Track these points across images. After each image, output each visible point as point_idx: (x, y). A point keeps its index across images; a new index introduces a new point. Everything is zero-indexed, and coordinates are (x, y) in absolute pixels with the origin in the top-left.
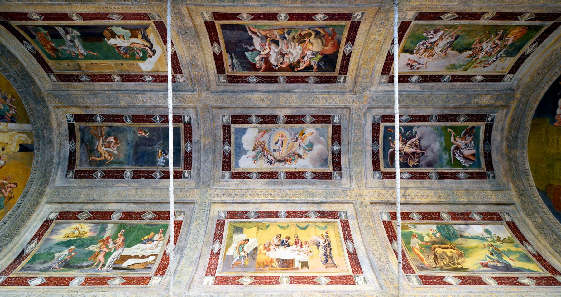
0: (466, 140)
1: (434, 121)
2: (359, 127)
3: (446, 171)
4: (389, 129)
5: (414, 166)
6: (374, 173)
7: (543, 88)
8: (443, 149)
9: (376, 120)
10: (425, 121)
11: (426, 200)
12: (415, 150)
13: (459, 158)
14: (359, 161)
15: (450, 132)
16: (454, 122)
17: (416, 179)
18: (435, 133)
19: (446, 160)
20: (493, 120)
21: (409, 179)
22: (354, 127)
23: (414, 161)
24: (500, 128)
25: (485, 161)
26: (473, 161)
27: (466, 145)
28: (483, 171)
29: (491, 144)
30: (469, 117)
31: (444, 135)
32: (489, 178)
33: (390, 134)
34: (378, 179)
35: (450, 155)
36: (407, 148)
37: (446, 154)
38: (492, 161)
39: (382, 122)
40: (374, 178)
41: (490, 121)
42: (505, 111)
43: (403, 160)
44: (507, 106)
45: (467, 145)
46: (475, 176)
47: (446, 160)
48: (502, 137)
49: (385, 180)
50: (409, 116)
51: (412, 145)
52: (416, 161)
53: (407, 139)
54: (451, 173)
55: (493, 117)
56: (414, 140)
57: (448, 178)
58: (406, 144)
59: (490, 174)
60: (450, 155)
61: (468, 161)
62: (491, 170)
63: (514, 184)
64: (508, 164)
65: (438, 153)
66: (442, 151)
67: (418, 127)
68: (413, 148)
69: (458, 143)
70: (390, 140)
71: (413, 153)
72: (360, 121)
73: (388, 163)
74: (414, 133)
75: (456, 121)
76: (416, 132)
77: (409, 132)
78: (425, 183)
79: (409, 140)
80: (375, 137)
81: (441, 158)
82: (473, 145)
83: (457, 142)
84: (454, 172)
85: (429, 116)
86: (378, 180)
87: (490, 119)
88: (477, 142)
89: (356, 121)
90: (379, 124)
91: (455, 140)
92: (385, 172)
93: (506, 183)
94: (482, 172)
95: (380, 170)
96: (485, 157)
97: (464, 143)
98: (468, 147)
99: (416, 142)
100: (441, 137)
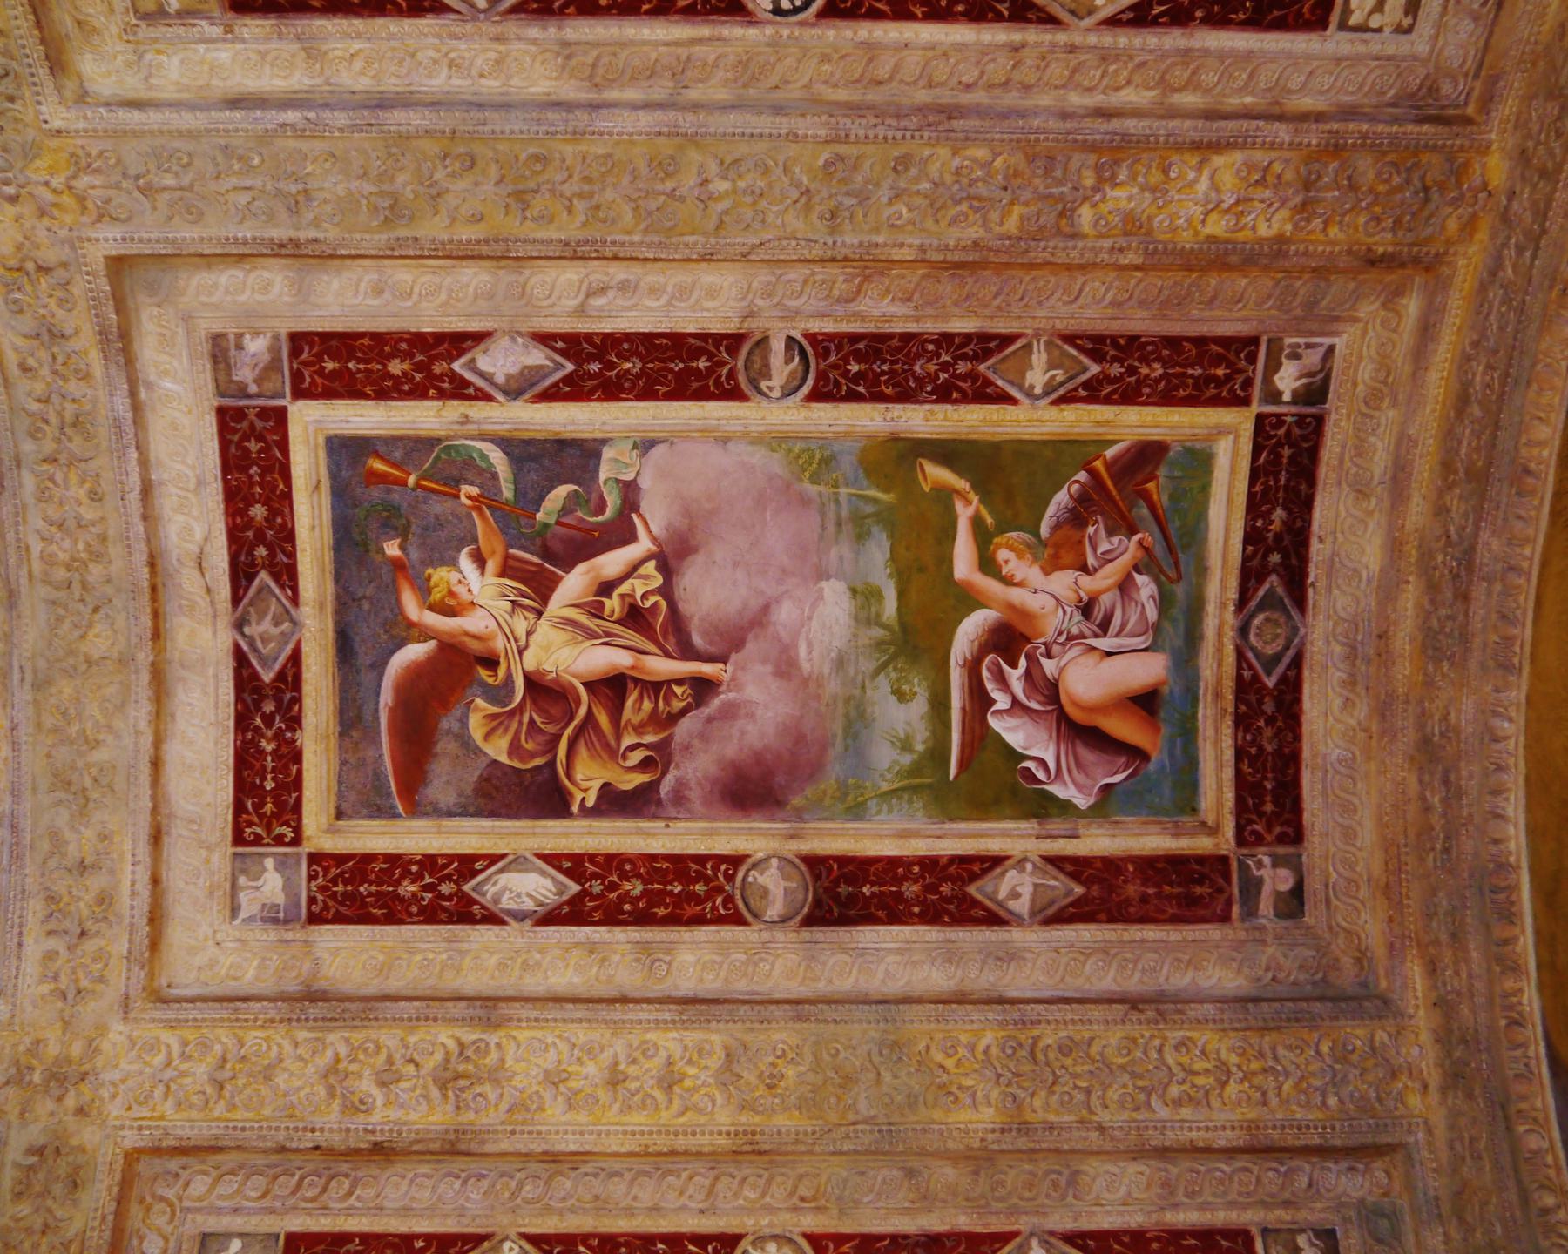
0: (1084, 568)
1: (788, 392)
2: (76, 445)
3: (889, 849)
4: (378, 465)
5: (614, 803)
6: (242, 867)
8: (879, 645)
9: (245, 374)
10: (702, 395)
12: (620, 659)
13: (1014, 732)
14: (100, 756)
15: (945, 496)
16: (965, 399)
17: (612, 917)
18: (805, 501)
19: (906, 745)
20: (1315, 392)
21: (551, 918)
22: (27, 447)
23: (613, 754)
24: (1380, 463)
25: (1240, 754)
26: (1136, 754)
27: (1086, 609)
28: (1203, 844)
29: (1301, 603)
30: (1096, 355)
31: (885, 517)
32: (1251, 912)
33: (393, 510)
34: (273, 917)
35: (939, 704)
36: (560, 636)
37: (901, 696)
38: (1294, 759)
39: (299, 393)
40: (235, 911)
41: (1298, 398)
43: (515, 749)
45: (1098, 614)
46: (1132, 890)
47: (906, 745)
48: (1395, 547)
49: (330, 937)
50: (544, 339)
51: (596, 611)
52: (636, 757)
53: (547, 554)
54: (930, 864)
55: (1313, 359)
56: (612, 562)
57: (892, 912)
58: (544, 599)
59: (1266, 873)
60: (939, 704)
61: (1087, 755)
62: (1282, 839)
65: (833, 687)
66: (868, 665)
67: (645, 446)
68: (608, 640)
69: (1016, 595)
70: (398, 565)
71: (612, 687)
72: (74, 387)
73: (378, 775)
74: (613, 501)
75: (985, 394)
76: (630, 492)
77: (562, 491)
78: (686, 957)
79: (569, 566)
80: (260, 538)
81: (857, 720)
82: (1152, 613)
83: (1008, 581)
84: (954, 859)
85: (733, 341)
86: (272, 934)
87: (1287, 380)
88: (1180, 590)
89: (39, 388)
90: (280, 417)
91: (987, 564)
92: (340, 859)
93: (1380, 952)
94: (1201, 859)
95: (296, 841)
96: (1241, 722)
97: (1067, 595)
98: (1104, 627)
99: (636, 587)
100: (861, 536)
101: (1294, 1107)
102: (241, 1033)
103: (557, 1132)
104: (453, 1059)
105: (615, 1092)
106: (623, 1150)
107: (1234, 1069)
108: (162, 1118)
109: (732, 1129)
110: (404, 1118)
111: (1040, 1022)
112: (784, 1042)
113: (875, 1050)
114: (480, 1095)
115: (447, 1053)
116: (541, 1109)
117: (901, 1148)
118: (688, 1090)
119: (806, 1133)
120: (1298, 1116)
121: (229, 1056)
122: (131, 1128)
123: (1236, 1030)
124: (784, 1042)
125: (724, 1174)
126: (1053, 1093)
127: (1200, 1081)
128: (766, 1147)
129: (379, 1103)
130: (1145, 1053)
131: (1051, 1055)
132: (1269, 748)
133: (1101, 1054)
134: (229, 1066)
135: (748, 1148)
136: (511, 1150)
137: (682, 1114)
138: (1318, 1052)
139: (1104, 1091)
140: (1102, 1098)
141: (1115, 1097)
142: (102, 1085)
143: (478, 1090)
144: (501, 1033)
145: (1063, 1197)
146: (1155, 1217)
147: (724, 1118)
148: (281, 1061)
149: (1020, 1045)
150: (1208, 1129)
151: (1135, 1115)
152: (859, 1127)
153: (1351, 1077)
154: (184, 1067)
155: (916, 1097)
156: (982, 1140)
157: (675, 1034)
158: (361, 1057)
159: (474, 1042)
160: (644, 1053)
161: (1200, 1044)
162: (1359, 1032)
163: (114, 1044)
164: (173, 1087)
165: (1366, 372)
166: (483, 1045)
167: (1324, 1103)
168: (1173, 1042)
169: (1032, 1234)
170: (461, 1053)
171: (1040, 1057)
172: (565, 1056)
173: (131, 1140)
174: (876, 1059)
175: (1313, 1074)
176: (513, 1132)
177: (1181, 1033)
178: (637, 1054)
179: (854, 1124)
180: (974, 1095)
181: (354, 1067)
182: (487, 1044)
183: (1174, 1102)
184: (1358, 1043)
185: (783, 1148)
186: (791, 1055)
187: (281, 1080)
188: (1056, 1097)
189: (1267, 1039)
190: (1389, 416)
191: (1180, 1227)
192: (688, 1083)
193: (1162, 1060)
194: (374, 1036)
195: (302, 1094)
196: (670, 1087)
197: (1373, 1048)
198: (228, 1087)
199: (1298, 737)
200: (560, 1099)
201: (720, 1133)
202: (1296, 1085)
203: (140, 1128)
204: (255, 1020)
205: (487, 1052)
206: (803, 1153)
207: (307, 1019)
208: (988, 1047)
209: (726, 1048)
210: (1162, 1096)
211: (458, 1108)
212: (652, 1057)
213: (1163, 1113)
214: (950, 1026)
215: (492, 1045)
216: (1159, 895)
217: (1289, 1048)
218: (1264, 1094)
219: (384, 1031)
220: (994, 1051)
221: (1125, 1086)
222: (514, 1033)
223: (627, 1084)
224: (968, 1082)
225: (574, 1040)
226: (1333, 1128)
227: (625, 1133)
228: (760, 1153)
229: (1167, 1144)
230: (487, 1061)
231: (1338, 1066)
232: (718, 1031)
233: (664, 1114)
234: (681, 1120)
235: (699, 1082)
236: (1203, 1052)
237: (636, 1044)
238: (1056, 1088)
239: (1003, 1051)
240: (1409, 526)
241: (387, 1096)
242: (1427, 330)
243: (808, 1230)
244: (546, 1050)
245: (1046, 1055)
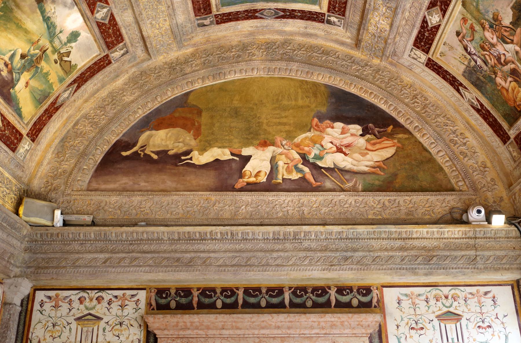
7: (386, 102)
32: (198, 20)
42: (349, 41)
44: (358, 43)
48: (292, 34)
63: (193, 55)
64: (234, 43)
127: (157, 25)
132: (240, 16)
165: (334, 32)
190: (323, 33)
199: (243, 20)
216: (200, 4)
240: (296, 37)
242: (343, 43)
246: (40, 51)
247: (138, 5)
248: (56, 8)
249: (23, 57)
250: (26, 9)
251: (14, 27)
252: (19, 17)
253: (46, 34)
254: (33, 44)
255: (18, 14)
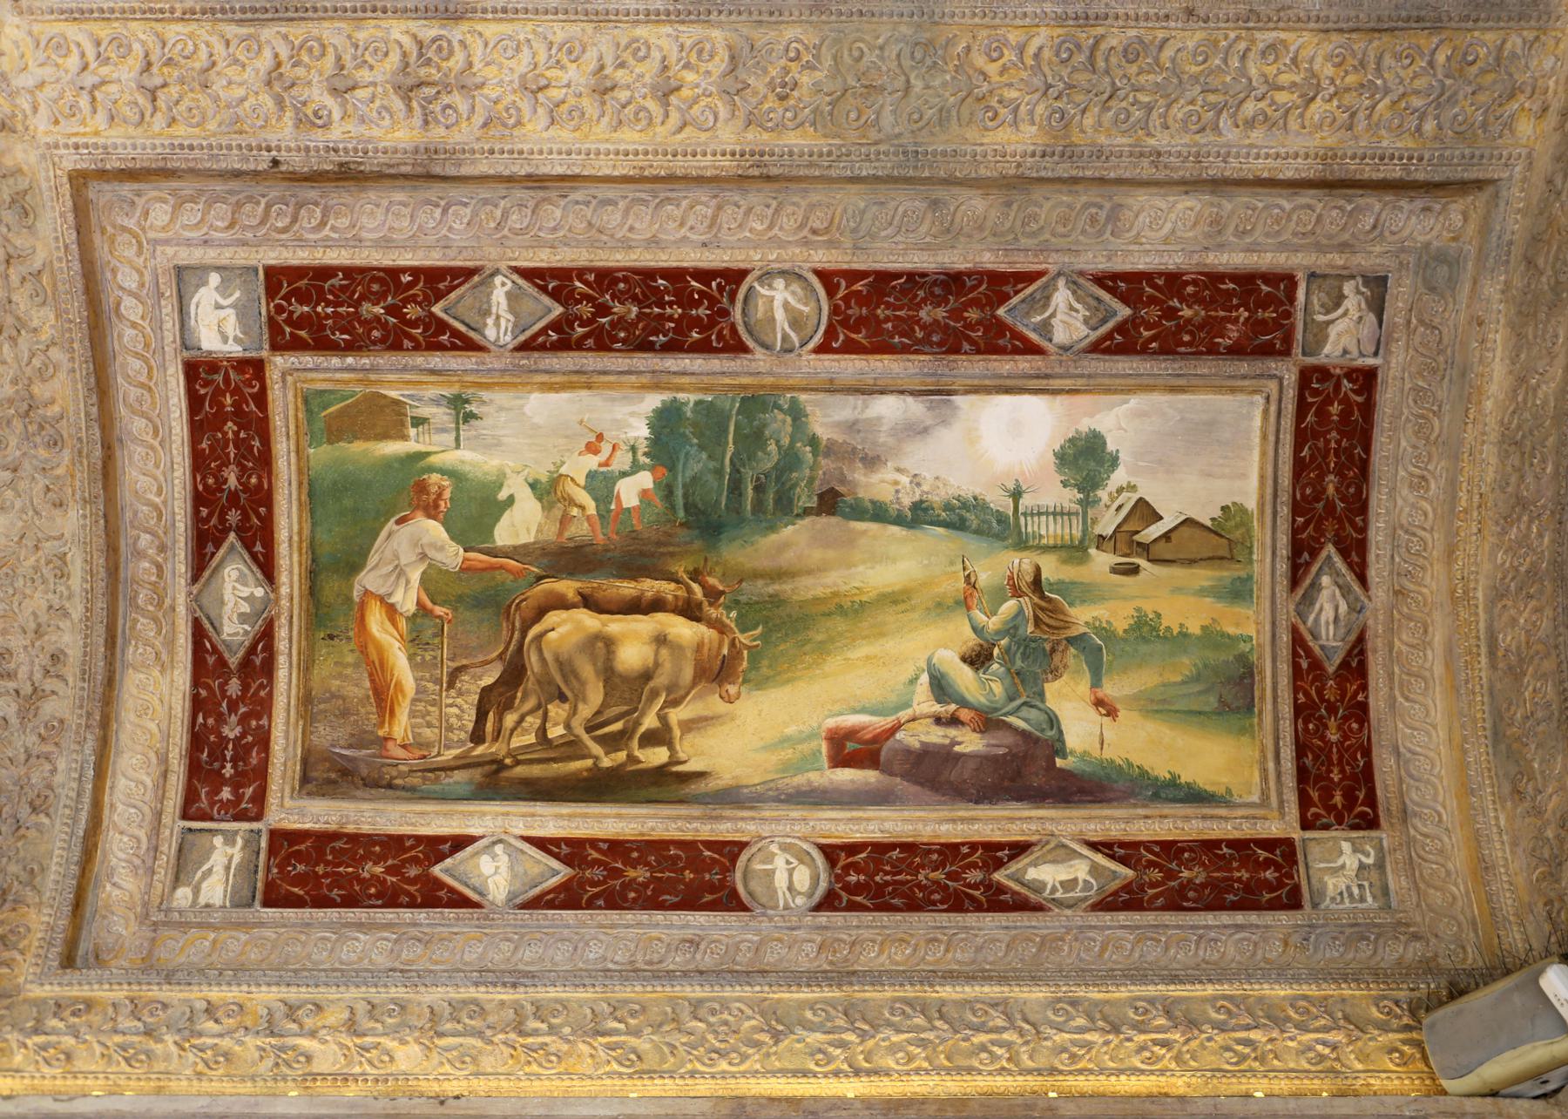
11: (630, 138)
101: (1383, 132)
102: (159, 27)
103: (541, 152)
104: (413, 58)
105: (603, 103)
106: (616, 173)
107: (1325, 83)
108: (97, 133)
109: (738, 148)
110: (367, 133)
111: (1106, 17)
112: (798, 41)
113: (907, 51)
114: (449, 106)
115: (405, 55)
116: (519, 123)
117: (926, 174)
118: (684, 101)
119: (821, 155)
120: (1385, 144)
121: (153, 58)
122: (66, 146)
123: (1341, 31)
124: (798, 41)
125: (728, 202)
126: (1109, 109)
128: (774, 171)
129: (336, 115)
130: (1225, 61)
131: (1113, 60)
133: (1173, 60)
134: (155, 69)
135: (756, 172)
136: (492, 172)
137: (681, 129)
138: (1431, 64)
139: (1169, 106)
140: (1164, 116)
141: (1180, 115)
142: (18, 92)
143: (446, 100)
144: (465, 26)
145: (1100, 233)
146: (1196, 258)
147: (728, 136)
148: (214, 64)
149: (1079, 47)
150: (1278, 156)
151: (1197, 137)
152: (882, 148)
153: (1461, 95)
154: (104, 71)
155: (949, 111)
156: (1019, 165)
157: (668, 29)
158: (306, 59)
159: (434, 41)
160: (634, 54)
161: (1292, 49)
162: (1490, 37)
163: (16, 43)
164: (97, 93)
166: (445, 44)
167: (1419, 129)
168: (1261, 46)
169: (1059, 274)
170: (421, 55)
171: (1101, 64)
172: (542, 57)
173: (70, 162)
174: (907, 63)
175: (1417, 92)
176: (492, 152)
177: (1274, 34)
178: (627, 56)
179: (876, 143)
180: (1016, 111)
181: (300, 71)
182: (449, 42)
183: (1246, 122)
184: (1483, 52)
185: (794, 173)
186: (806, 57)
187: (218, 86)
188: (1111, 114)
189: (1376, 43)
191: (1221, 269)
192: (685, 92)
193: (1243, 71)
194: (315, 32)
195: (247, 104)
196: (665, 95)
197: (1498, 59)
198: (160, 94)
200: (540, 111)
201: (724, 154)
202: (1394, 103)
203: (77, 147)
204: (172, 11)
205: (451, 53)
206: (815, 178)
207: (233, 10)
208: (1040, 49)
209: (730, 48)
210: (1234, 116)
211: (426, 122)
212: (645, 58)
213: (1231, 134)
214: (997, 21)
215: (456, 44)
217: (1398, 57)
218: (1353, 115)
219: (326, 24)
220: (1047, 54)
221: (1192, 102)
222: (479, 27)
223: (616, 93)
224: (1014, 94)
225: (550, 37)
226: (1421, 159)
227: (617, 153)
228: (768, 178)
229: (1227, 174)
230: (451, 63)
231: (1448, 82)
232: (720, 25)
233: (659, 129)
234: (679, 137)
235: (699, 91)
236: (1294, 61)
237: (624, 42)
238: (1111, 103)
239: (1057, 55)
241: (344, 105)
243: (819, 266)
244: (518, 49)
245: (1107, 60)
246: (1017, 593)
247: (1099, 153)
248: (905, 463)
249: (977, 659)
250: (817, 555)
251: (840, 624)
252: (819, 592)
253: (971, 543)
254: (965, 603)
255: (808, 588)
